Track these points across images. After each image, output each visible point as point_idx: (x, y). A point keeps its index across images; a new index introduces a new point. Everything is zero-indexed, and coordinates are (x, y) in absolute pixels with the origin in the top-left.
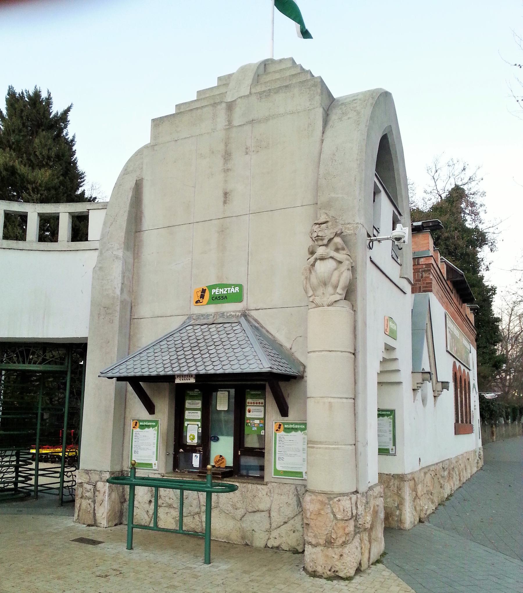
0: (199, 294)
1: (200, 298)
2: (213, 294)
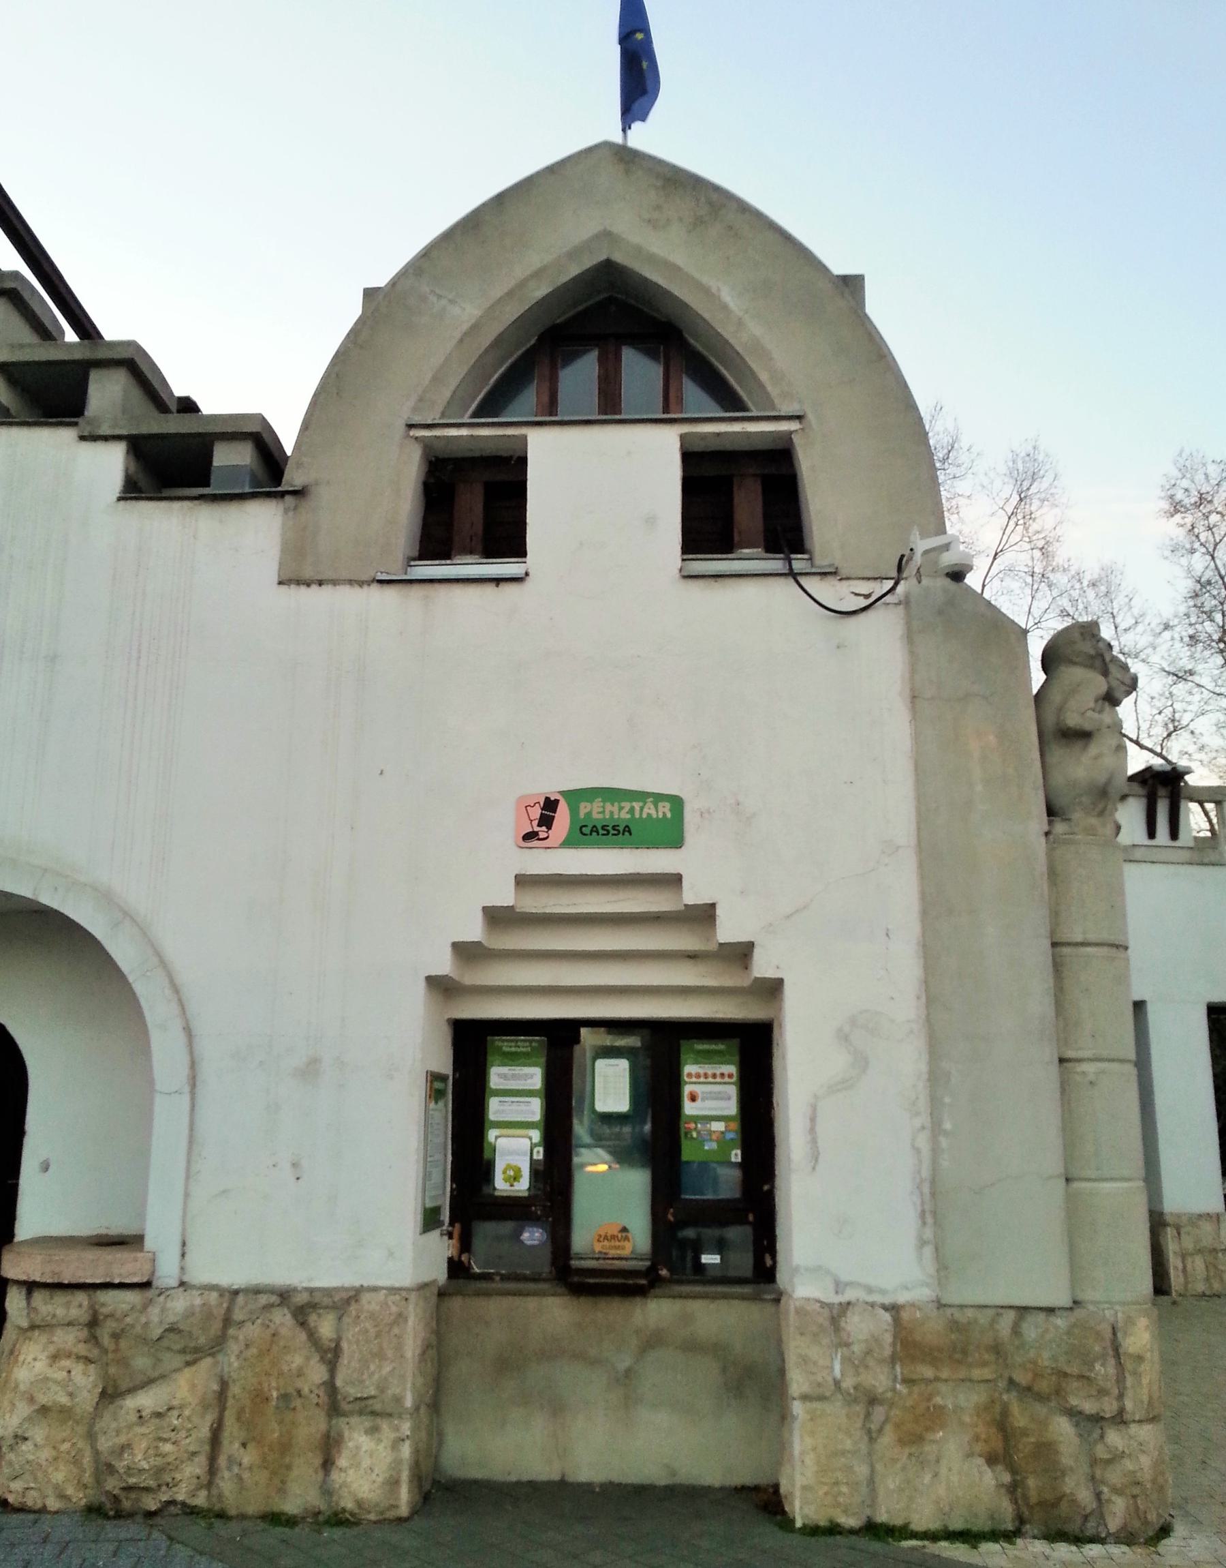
0: (536, 813)
2: (582, 816)
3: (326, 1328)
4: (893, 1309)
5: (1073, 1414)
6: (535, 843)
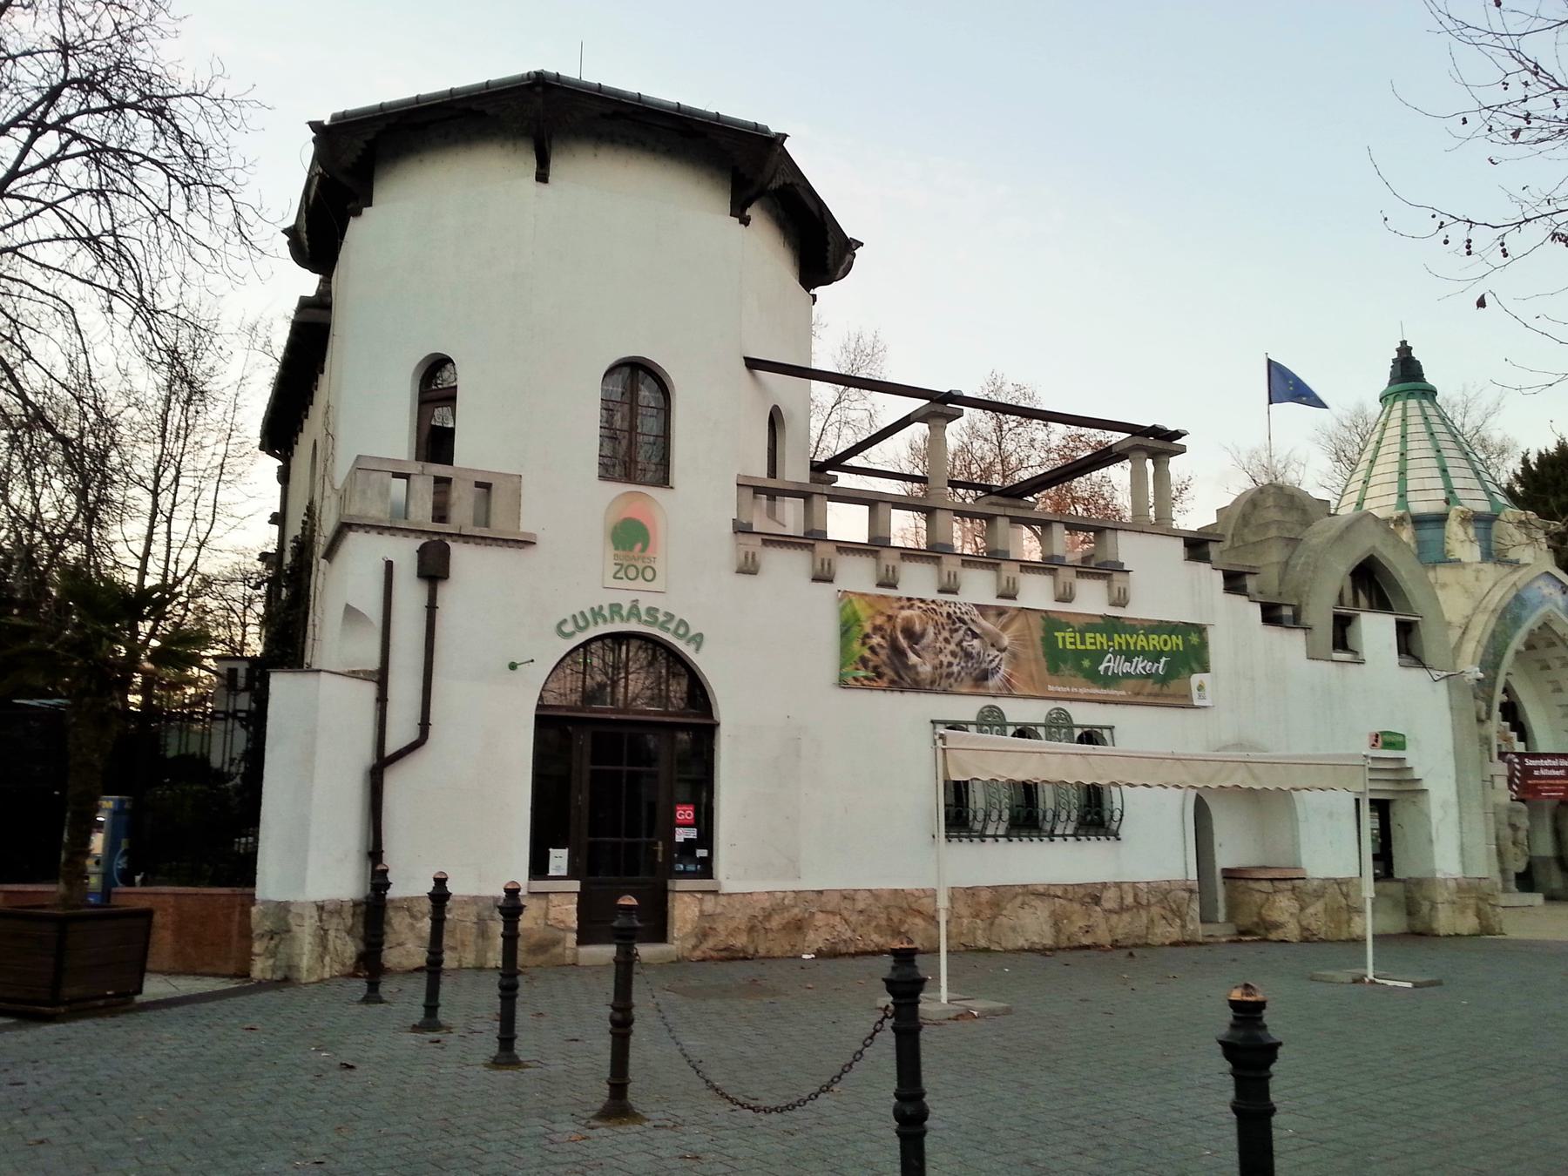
3: (1344, 889)
4: (1456, 879)
5: (1490, 904)
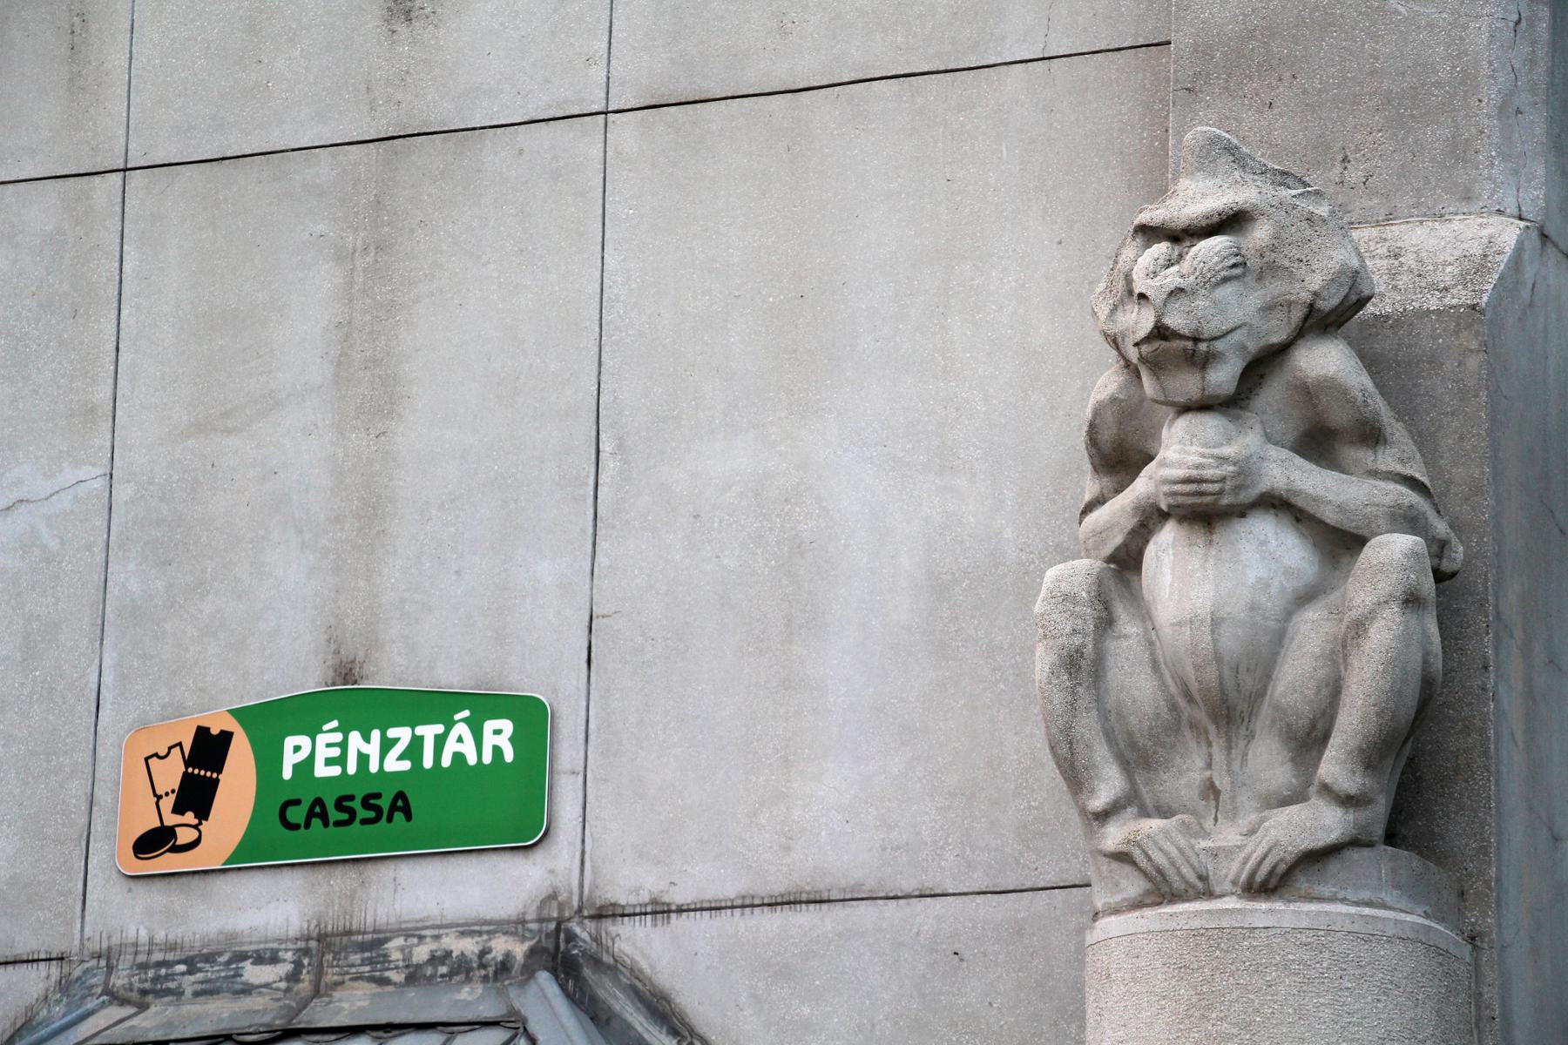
0: (171, 774)
1: (178, 809)
6: (167, 862)
